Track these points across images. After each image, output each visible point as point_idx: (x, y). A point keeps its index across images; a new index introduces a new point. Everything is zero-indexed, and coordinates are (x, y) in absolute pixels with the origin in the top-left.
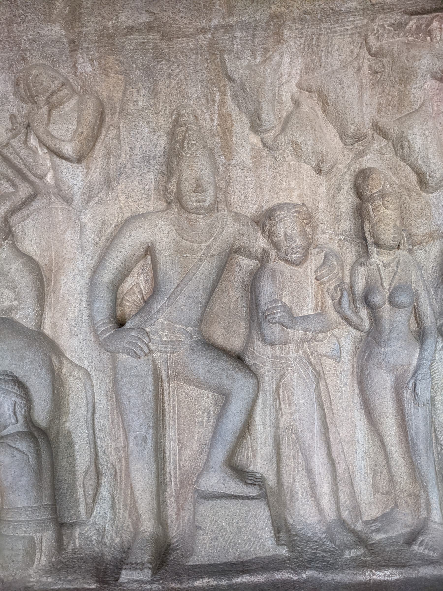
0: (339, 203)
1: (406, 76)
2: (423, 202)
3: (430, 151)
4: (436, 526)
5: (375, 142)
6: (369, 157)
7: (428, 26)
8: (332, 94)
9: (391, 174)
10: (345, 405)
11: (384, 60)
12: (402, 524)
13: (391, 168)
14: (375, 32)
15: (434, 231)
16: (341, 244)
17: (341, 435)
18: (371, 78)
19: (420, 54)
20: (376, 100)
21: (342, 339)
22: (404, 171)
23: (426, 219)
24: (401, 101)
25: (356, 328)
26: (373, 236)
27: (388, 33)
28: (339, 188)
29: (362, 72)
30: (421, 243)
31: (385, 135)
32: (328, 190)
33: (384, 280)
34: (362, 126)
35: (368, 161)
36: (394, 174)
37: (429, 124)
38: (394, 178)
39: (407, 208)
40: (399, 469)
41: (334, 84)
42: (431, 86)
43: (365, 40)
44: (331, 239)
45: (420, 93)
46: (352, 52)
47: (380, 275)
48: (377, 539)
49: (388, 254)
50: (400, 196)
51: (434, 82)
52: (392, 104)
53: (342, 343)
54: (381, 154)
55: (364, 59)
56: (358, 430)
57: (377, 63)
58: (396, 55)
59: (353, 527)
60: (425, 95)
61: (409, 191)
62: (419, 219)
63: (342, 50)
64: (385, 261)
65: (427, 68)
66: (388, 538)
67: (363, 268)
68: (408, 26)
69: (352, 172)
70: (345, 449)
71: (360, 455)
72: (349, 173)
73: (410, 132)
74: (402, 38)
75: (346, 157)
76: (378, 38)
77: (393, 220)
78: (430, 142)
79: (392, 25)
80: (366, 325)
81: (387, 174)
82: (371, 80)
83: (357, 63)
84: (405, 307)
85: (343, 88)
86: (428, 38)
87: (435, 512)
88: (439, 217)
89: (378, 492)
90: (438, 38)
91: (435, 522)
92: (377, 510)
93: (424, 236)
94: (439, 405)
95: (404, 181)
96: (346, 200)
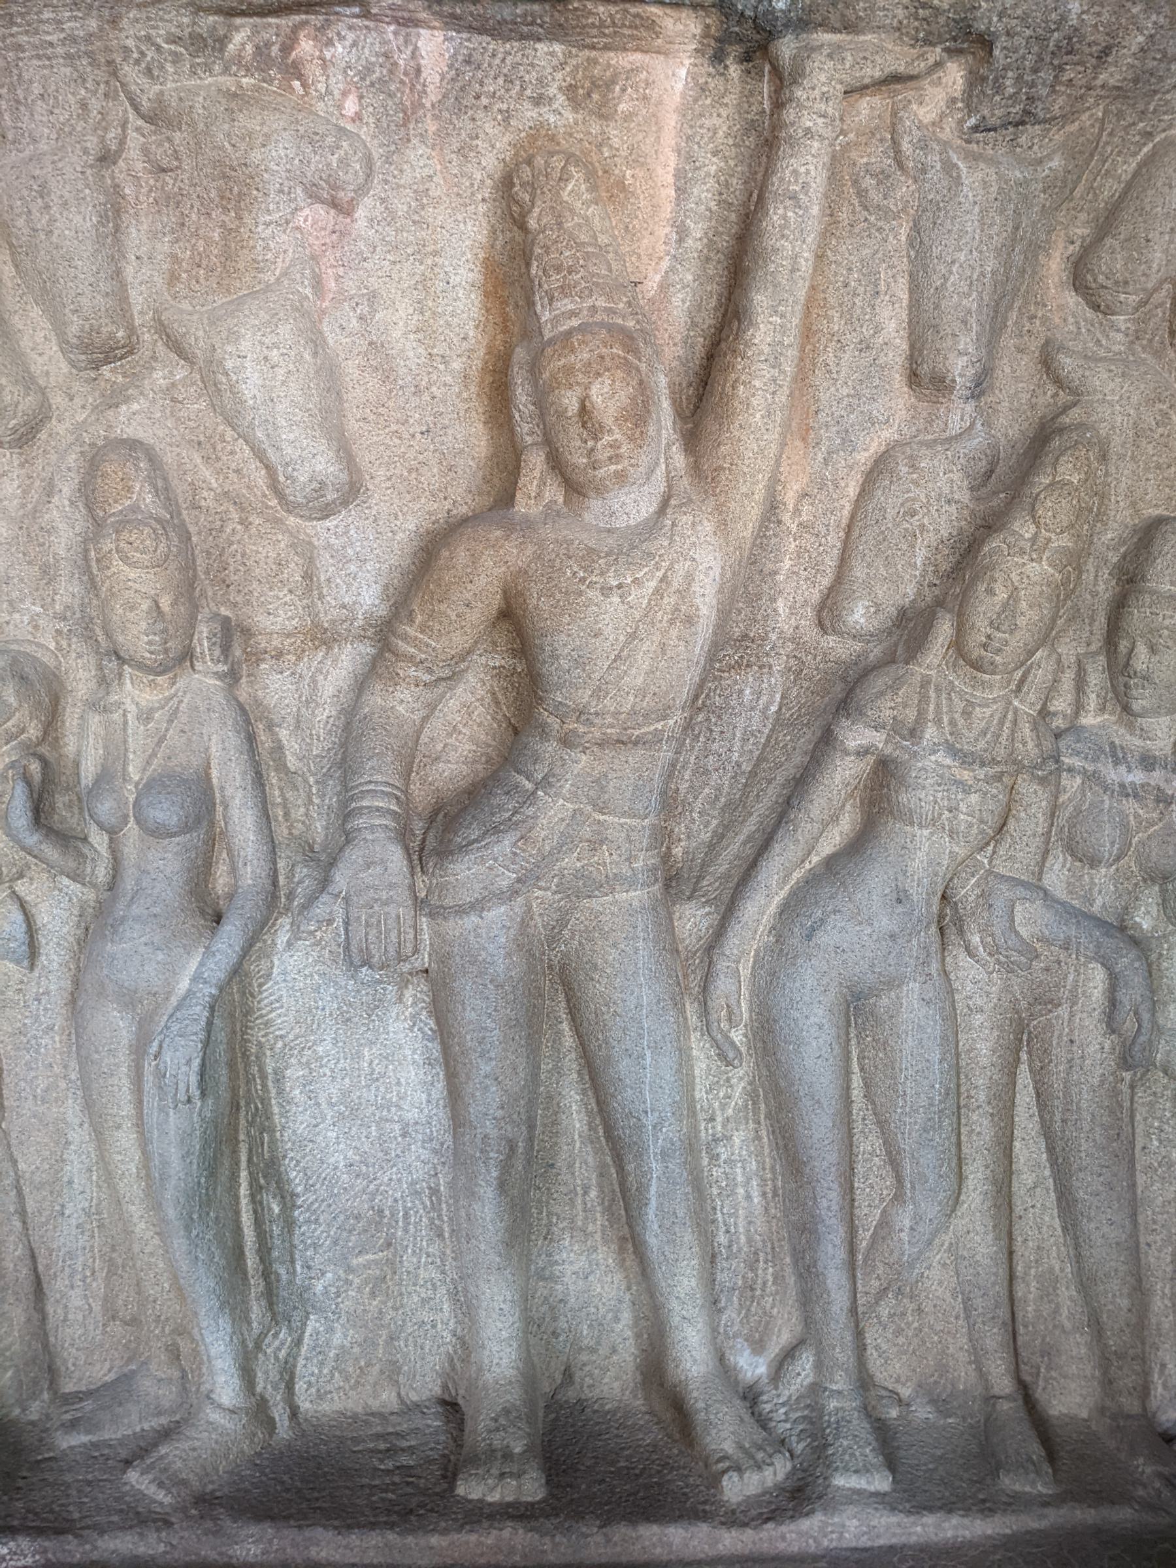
0: (50, 531)
1: (235, 189)
2: (282, 545)
3: (280, 407)
4: (215, 1416)
5: (158, 365)
6: (135, 406)
7: (286, 49)
8: (21, 222)
9: (199, 461)
10: (42, 1084)
11: (177, 136)
12: (147, 1405)
13: (199, 443)
14: (135, 55)
15: (333, 622)
16: (64, 643)
17: (22, 1166)
18: (152, 182)
19: (266, 129)
20: (164, 246)
21: (43, 907)
22: (232, 453)
23: (290, 591)
24: (228, 256)
25: (75, 877)
26: (108, 635)
27: (174, 62)
28: (50, 491)
29: (121, 163)
30: (279, 655)
31: (178, 348)
32: (24, 492)
33: (131, 756)
34: (104, 321)
35: (134, 420)
36: (206, 459)
37: (281, 330)
38: (206, 473)
39: (239, 557)
40: (149, 1264)
41: (25, 193)
42: (315, 223)
43: (114, 74)
44: (36, 627)
45: (284, 237)
46: (84, 105)
47: (125, 742)
48: (65, 1445)
49: (152, 684)
50: (219, 523)
51: (320, 209)
52: (204, 263)
53: (43, 917)
54: (173, 400)
55: (124, 125)
56: (71, 1155)
57: (160, 145)
58: (201, 126)
59: (17, 1411)
60: (297, 246)
61: (243, 510)
62: (271, 589)
63: (56, 98)
64: (144, 703)
65: (289, 171)
66: (95, 1445)
67: (97, 718)
68: (231, 46)
69: (87, 448)
70: (31, 1206)
71: (74, 1222)
72: (78, 449)
73: (229, 348)
74: (221, 79)
75: (78, 401)
76: (149, 71)
77: (145, 596)
78: (284, 383)
79: (174, 40)
80: (102, 873)
81: (186, 460)
82: (151, 191)
83: (95, 140)
84: (172, 835)
85: (47, 207)
86: (296, 84)
87: (221, 1379)
88: (349, 585)
89: (114, 1318)
90: (321, 87)
91: (219, 1406)
92: (107, 1365)
93: (288, 636)
94: (297, 1092)
95: (233, 483)
96: (64, 526)
